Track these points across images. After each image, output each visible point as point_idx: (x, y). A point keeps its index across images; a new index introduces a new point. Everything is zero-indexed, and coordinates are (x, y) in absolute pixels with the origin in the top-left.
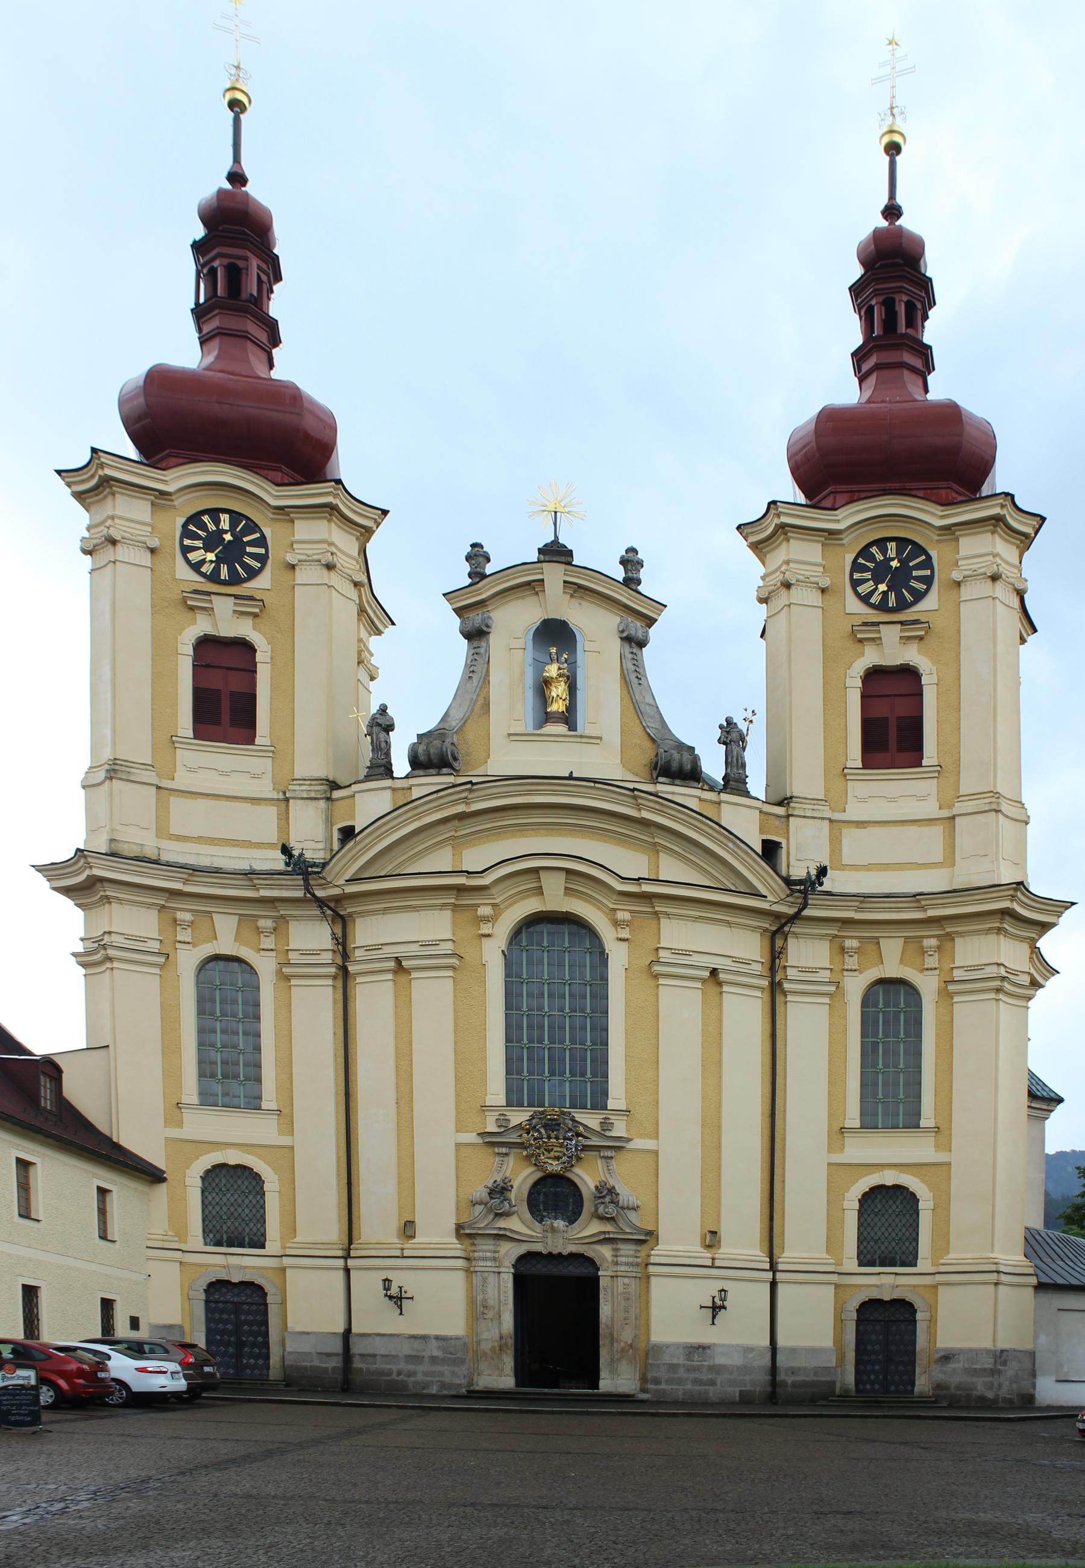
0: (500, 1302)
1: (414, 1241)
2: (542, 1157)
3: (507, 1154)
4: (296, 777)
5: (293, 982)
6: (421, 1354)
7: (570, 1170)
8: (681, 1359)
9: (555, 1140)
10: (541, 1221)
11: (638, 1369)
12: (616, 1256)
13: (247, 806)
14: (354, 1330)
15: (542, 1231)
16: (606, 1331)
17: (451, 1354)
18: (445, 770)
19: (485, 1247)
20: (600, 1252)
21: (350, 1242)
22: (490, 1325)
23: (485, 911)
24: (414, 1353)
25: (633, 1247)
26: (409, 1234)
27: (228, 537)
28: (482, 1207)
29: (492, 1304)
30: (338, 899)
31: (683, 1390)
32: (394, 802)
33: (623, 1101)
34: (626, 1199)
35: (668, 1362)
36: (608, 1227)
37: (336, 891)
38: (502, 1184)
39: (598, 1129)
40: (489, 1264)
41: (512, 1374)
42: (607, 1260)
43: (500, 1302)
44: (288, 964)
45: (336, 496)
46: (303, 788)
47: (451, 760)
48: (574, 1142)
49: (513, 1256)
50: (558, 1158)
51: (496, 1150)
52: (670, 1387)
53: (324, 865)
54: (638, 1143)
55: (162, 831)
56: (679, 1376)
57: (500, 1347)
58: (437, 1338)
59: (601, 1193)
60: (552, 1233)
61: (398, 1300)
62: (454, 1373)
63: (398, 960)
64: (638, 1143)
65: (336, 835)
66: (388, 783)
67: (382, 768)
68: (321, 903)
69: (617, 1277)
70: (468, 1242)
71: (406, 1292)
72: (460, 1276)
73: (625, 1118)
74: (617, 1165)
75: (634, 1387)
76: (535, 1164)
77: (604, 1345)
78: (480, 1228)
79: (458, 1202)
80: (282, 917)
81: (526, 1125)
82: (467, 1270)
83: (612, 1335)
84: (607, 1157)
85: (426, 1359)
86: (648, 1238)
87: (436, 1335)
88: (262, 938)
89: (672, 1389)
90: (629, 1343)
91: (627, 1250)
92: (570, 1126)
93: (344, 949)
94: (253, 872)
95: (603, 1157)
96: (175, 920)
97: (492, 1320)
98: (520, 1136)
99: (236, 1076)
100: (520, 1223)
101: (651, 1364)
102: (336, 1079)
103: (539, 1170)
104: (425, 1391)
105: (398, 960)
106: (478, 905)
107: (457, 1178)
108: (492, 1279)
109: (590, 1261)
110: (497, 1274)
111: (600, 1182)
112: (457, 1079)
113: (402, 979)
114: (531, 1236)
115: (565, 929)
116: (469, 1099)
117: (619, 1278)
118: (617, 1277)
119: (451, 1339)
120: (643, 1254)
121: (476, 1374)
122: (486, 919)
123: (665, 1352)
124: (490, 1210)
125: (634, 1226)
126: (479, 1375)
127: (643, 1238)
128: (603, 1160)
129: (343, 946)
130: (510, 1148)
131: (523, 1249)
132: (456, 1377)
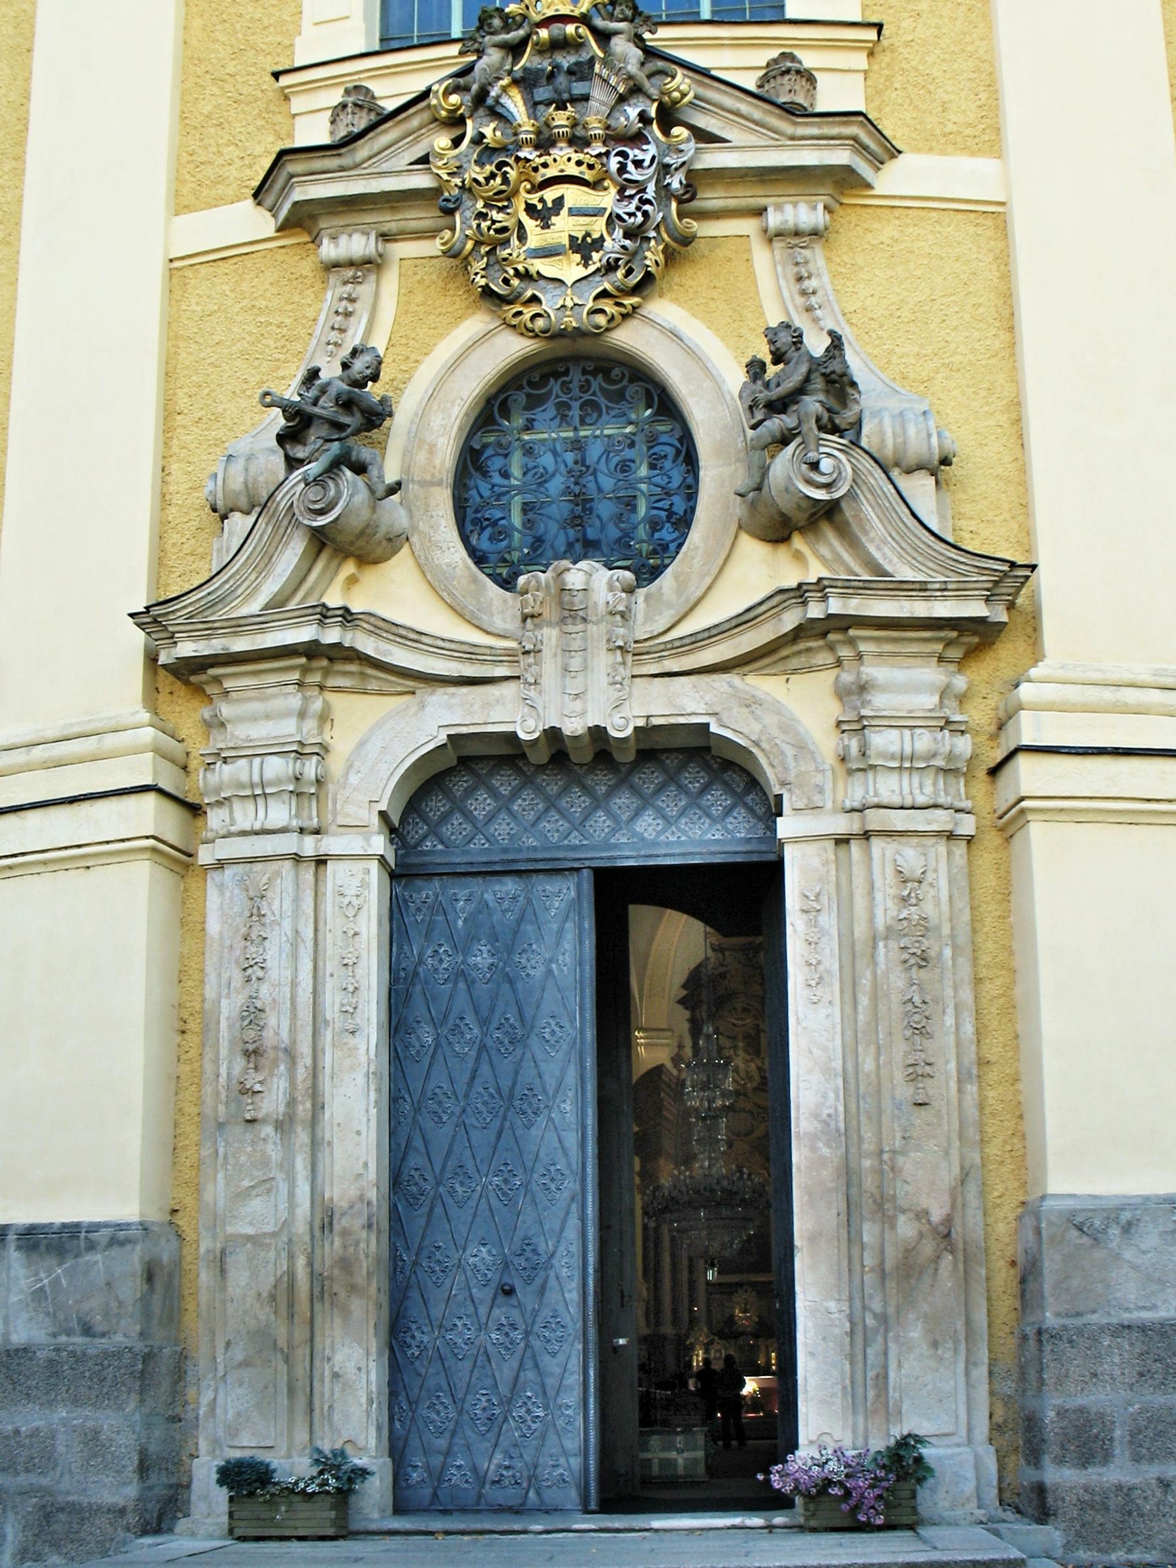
3: (370, 265)
9: (569, 152)
48: (652, 150)
49: (385, 769)
50: (584, 247)
78: (238, 626)
81: (447, 92)
84: (797, 233)
92: (633, 68)
95: (779, 234)
98: (424, 160)
111: (771, 335)
114: (470, 653)
120: (979, 714)
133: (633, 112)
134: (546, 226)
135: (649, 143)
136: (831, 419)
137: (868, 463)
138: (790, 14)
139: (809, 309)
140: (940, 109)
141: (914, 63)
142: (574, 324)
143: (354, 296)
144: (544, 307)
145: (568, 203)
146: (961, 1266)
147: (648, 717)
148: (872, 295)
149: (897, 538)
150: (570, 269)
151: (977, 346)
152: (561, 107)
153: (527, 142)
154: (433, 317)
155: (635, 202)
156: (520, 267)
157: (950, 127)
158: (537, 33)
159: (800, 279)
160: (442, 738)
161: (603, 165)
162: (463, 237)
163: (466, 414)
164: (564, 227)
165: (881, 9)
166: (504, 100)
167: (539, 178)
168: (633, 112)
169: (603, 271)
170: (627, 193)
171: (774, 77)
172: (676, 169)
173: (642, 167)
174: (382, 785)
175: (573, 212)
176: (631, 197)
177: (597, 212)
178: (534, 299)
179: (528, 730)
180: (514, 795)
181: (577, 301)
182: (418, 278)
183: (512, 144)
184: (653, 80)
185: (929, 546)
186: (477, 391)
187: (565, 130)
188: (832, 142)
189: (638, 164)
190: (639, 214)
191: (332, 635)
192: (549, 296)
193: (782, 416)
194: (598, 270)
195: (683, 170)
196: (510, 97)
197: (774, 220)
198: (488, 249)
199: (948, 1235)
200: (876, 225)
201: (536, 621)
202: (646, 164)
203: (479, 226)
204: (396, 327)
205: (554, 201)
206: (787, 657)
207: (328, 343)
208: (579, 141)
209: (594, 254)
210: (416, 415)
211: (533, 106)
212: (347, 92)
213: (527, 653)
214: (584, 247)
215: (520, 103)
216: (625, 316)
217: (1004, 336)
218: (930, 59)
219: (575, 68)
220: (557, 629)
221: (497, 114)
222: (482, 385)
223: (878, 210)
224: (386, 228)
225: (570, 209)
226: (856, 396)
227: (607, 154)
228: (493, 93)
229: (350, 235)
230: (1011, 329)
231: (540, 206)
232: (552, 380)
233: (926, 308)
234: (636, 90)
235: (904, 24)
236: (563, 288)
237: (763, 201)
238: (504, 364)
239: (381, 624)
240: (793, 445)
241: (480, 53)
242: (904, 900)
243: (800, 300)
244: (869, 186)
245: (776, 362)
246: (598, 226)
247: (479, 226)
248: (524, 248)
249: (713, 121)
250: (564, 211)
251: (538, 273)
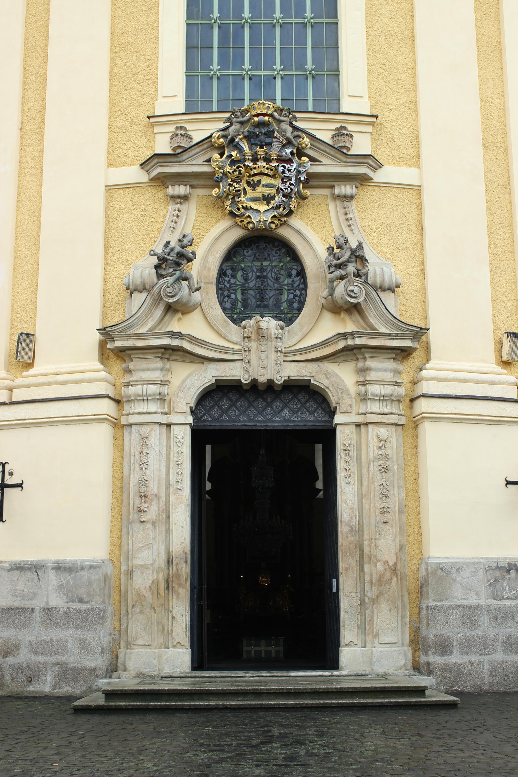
0: (168, 485)
1: (31, 372)
2: (243, 198)
6: (28, 604)
7: (285, 223)
8: (483, 596)
11: (407, 620)
12: (364, 383)
15: (239, 339)
16: (351, 538)
17: (81, 601)
20: (337, 375)
22: (152, 535)
24: (17, 604)
25: (390, 364)
26: (24, 357)
28: (144, 295)
29: (156, 491)
31: (490, 663)
33: (366, 99)
34: (379, 272)
35: (459, 602)
36: (350, 327)
38: (178, 249)
40: (152, 407)
41: (186, 642)
42: (348, 393)
43: (168, 485)
50: (267, 199)
51: (171, 191)
52: (466, 659)
56: (478, 632)
57: (167, 581)
59: (339, 259)
60: (258, 340)
62: (84, 645)
69: (366, 424)
70: (118, 366)
71: (11, 474)
73: (369, 129)
74: (359, 211)
75: (402, 663)
76: (231, 213)
77: (347, 569)
78: (139, 336)
83: (361, 548)
84: (345, 197)
85: (38, 615)
87: (57, 562)
89: (471, 663)
90: (391, 563)
95: (339, 196)
97: (153, 523)
98: (209, 160)
101: (433, 608)
103: (237, 224)
104: (31, 688)
107: (106, 248)
110: (164, 429)
112: (113, 77)
116: (129, 109)
117: (370, 427)
118: (366, 424)
119: (82, 568)
120: (405, 379)
121: (122, 644)
123: (455, 580)
126: (128, 645)
127: (407, 343)
128: (338, 203)
130: (192, 187)
133: (288, 151)
134: (254, 190)
135: (293, 163)
136: (358, 273)
137: (371, 289)
138: (343, 110)
139: (349, 226)
140: (398, 148)
141: (389, 130)
142: (263, 227)
143: (180, 209)
144: (252, 220)
145: (263, 182)
146: (399, 581)
147: (289, 376)
148: (372, 220)
149: (380, 316)
150: (263, 208)
151: (409, 240)
152: (262, 147)
153: (248, 159)
154: (209, 218)
155: (288, 184)
156: (244, 205)
157: (401, 155)
158: (253, 119)
159: (346, 214)
160: (214, 381)
161: (276, 170)
162: (223, 191)
163: (222, 257)
164: (260, 191)
165: (377, 107)
166: (240, 143)
167: (252, 173)
168: (288, 151)
169: (275, 208)
170: (284, 181)
171: (338, 136)
172: (303, 173)
173: (291, 172)
174: (191, 397)
175: (264, 186)
176: (286, 182)
177: (273, 186)
178: (249, 217)
179: (245, 380)
180: (237, 401)
181: (265, 219)
182: (204, 203)
183: (243, 159)
184: (296, 139)
185: (392, 321)
186: (226, 248)
187: (263, 156)
188: (359, 164)
189: (289, 170)
190: (289, 189)
192: (254, 215)
193: (341, 270)
194: (273, 207)
195: (305, 173)
196: (242, 142)
197: (337, 191)
198: (232, 197)
199: (395, 570)
200: (374, 193)
201: (249, 339)
202: (292, 171)
203: (229, 188)
204: (196, 222)
205: (257, 181)
206: (339, 356)
207: (171, 227)
208: (268, 160)
209: (271, 201)
210: (203, 256)
211: (251, 145)
212: (177, 128)
213: (245, 351)
214: (267, 199)
215: (246, 144)
216: (281, 225)
217: (419, 237)
218: (395, 128)
219: (267, 133)
220: (257, 343)
221: (238, 147)
222: (228, 246)
223: (374, 187)
224: (192, 183)
225: (263, 185)
226: (367, 264)
227: (278, 166)
228: (237, 140)
229: (179, 185)
230: (422, 234)
231: (252, 183)
232: (253, 245)
233: (391, 226)
234: (289, 143)
235: (385, 114)
236: (260, 213)
237: (333, 183)
238: (236, 239)
239: (192, 338)
240: (344, 281)
241: (232, 124)
242: (380, 448)
243: (346, 223)
244: (372, 179)
245: (338, 248)
246: (273, 191)
247: (229, 188)
248: (246, 198)
249: (316, 153)
250: (261, 185)
251: (250, 207)
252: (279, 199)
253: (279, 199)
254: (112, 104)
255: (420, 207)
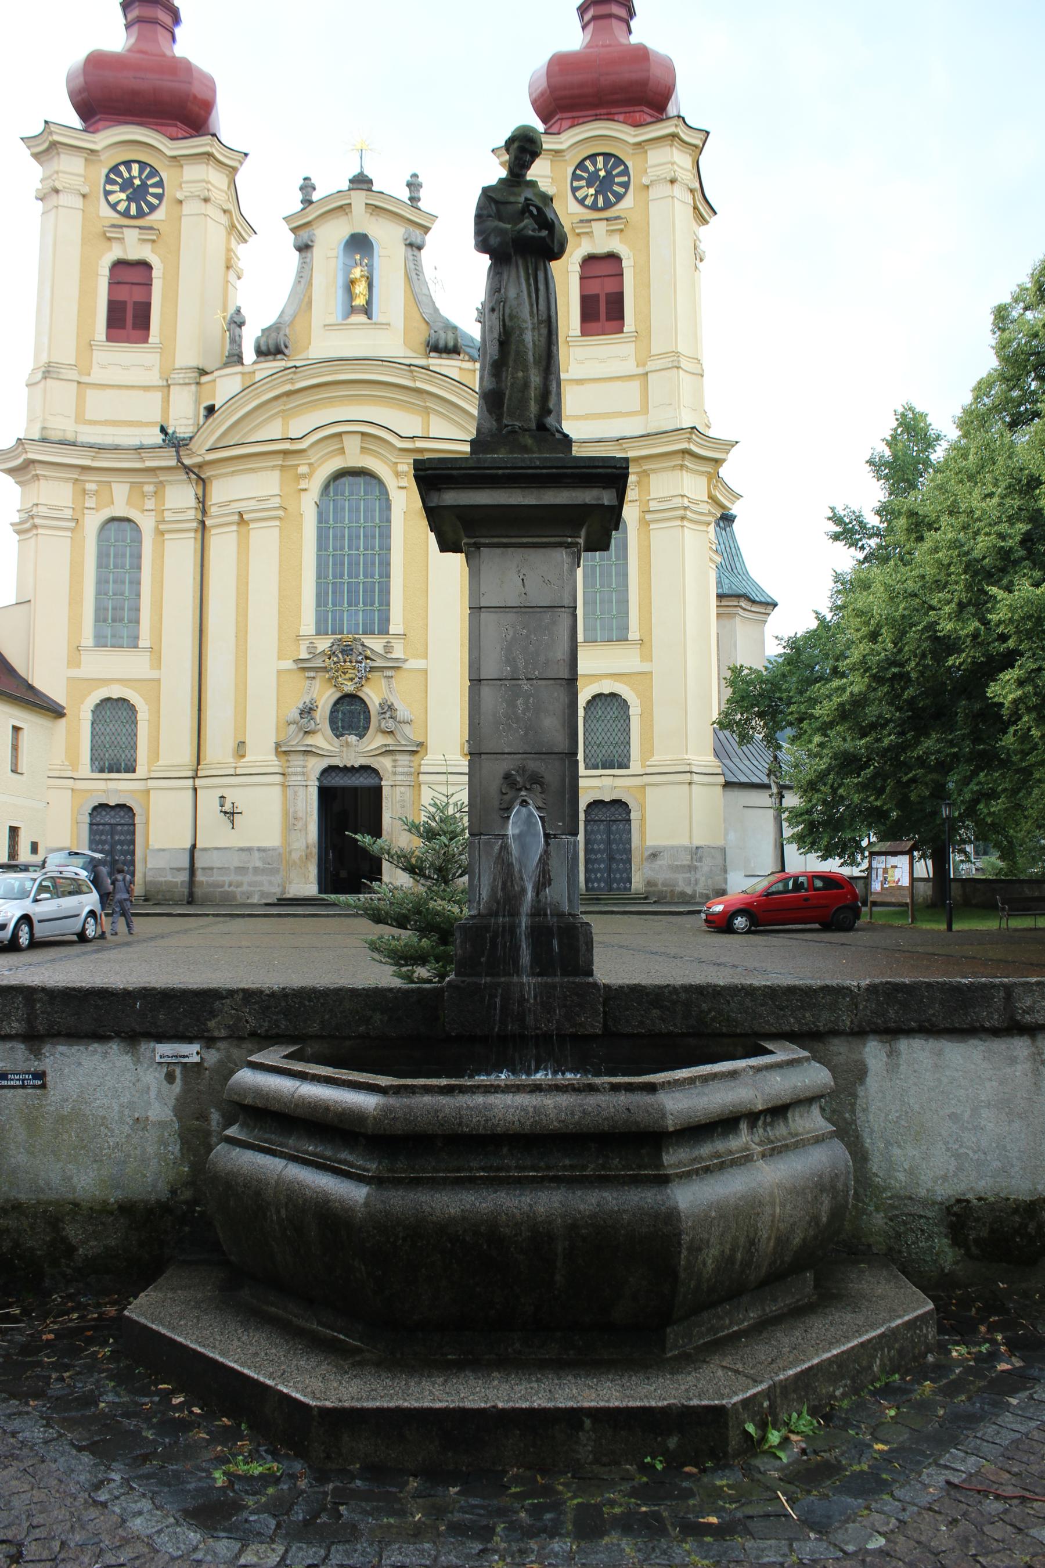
4: (177, 367)
5: (167, 536)
10: (337, 737)
13: (141, 393)
14: (198, 846)
18: (279, 357)
19: (297, 761)
21: (198, 764)
23: (303, 469)
27: (137, 182)
30: (200, 466)
32: (243, 383)
36: (389, 740)
37: (199, 460)
39: (381, 652)
40: (299, 778)
44: (164, 521)
45: (212, 146)
46: (181, 376)
47: (283, 346)
51: (307, 674)
53: (191, 438)
54: (413, 663)
55: (80, 418)
58: (259, 849)
61: (231, 815)
63: (240, 514)
64: (413, 663)
65: (202, 412)
66: (238, 369)
67: (236, 358)
68: (188, 469)
70: (284, 758)
72: (278, 789)
79: (278, 722)
80: (161, 482)
82: (284, 786)
86: (417, 750)
88: (146, 501)
91: (403, 759)
93: (204, 507)
94: (141, 448)
96: (84, 490)
99: (121, 620)
100: (323, 740)
102: (194, 618)
105: (240, 514)
106: (298, 465)
108: (301, 792)
109: (375, 771)
113: (243, 529)
114: (331, 751)
115: (360, 480)
120: (415, 764)
122: (303, 476)
124: (301, 729)
125: (408, 739)
129: (202, 503)
131: (325, 763)
132: (271, 888)
164: (348, 676)
191: (309, 749)
208: (351, 662)
214: (352, 679)
221: (337, 656)
252: (357, 679)
253: (357, 679)
254: (280, 627)
255: (426, 679)
